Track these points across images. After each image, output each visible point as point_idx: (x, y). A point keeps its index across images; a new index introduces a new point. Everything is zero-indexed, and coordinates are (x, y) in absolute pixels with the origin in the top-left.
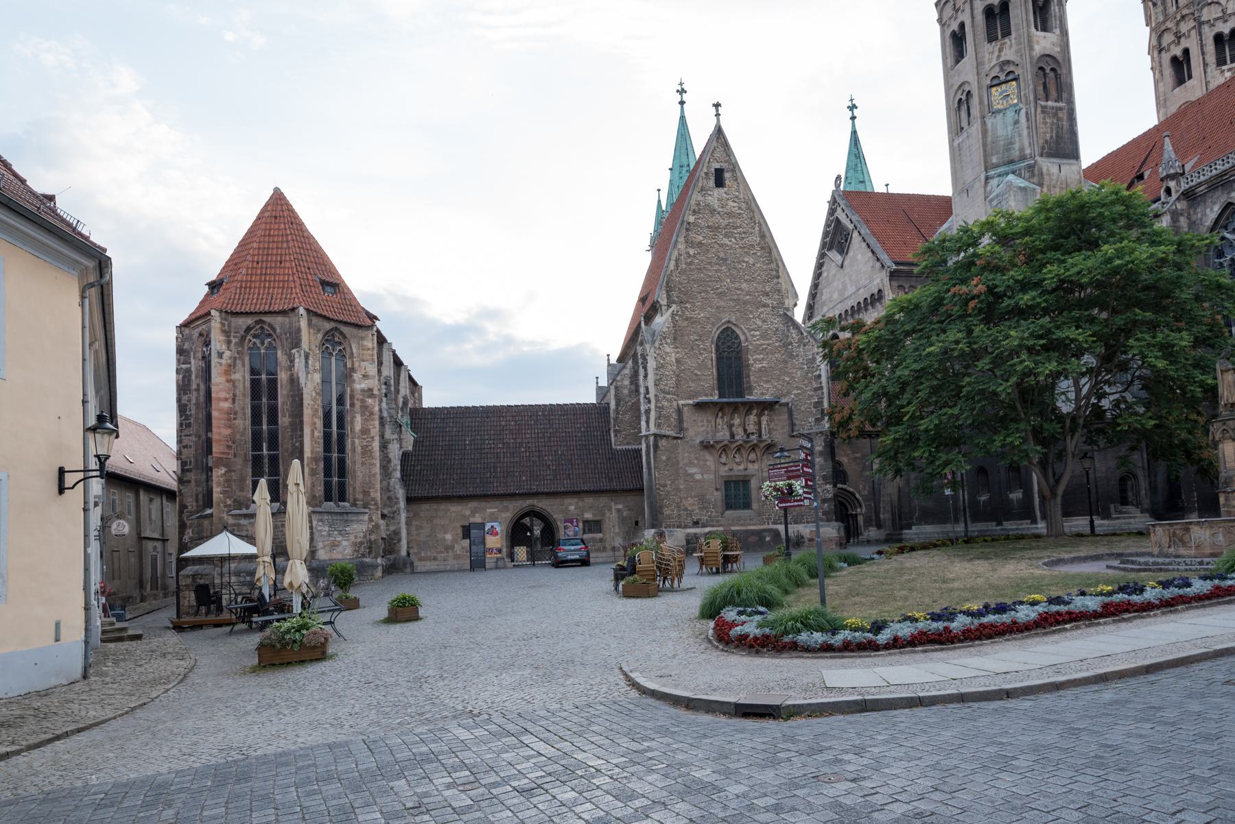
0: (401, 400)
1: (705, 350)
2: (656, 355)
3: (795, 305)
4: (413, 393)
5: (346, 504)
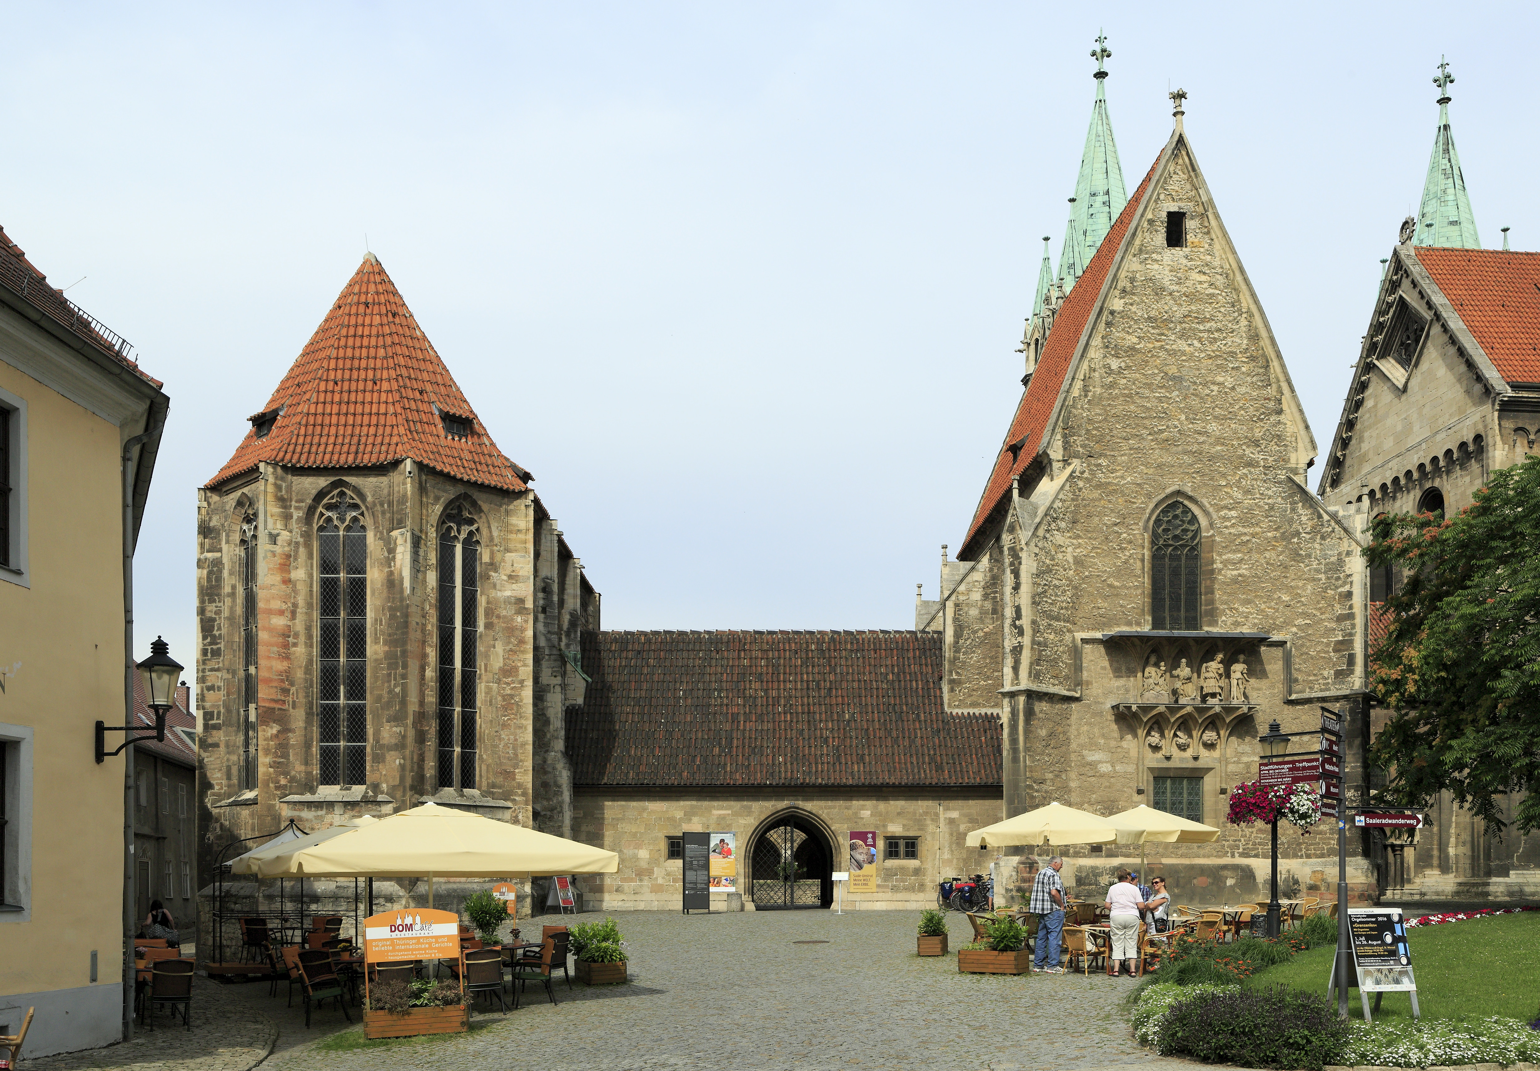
0: (566, 618)
1: (1130, 542)
2: (1037, 550)
3: (1311, 464)
4: (584, 605)
5: (475, 792)
